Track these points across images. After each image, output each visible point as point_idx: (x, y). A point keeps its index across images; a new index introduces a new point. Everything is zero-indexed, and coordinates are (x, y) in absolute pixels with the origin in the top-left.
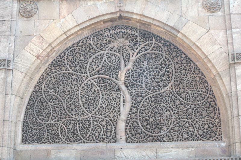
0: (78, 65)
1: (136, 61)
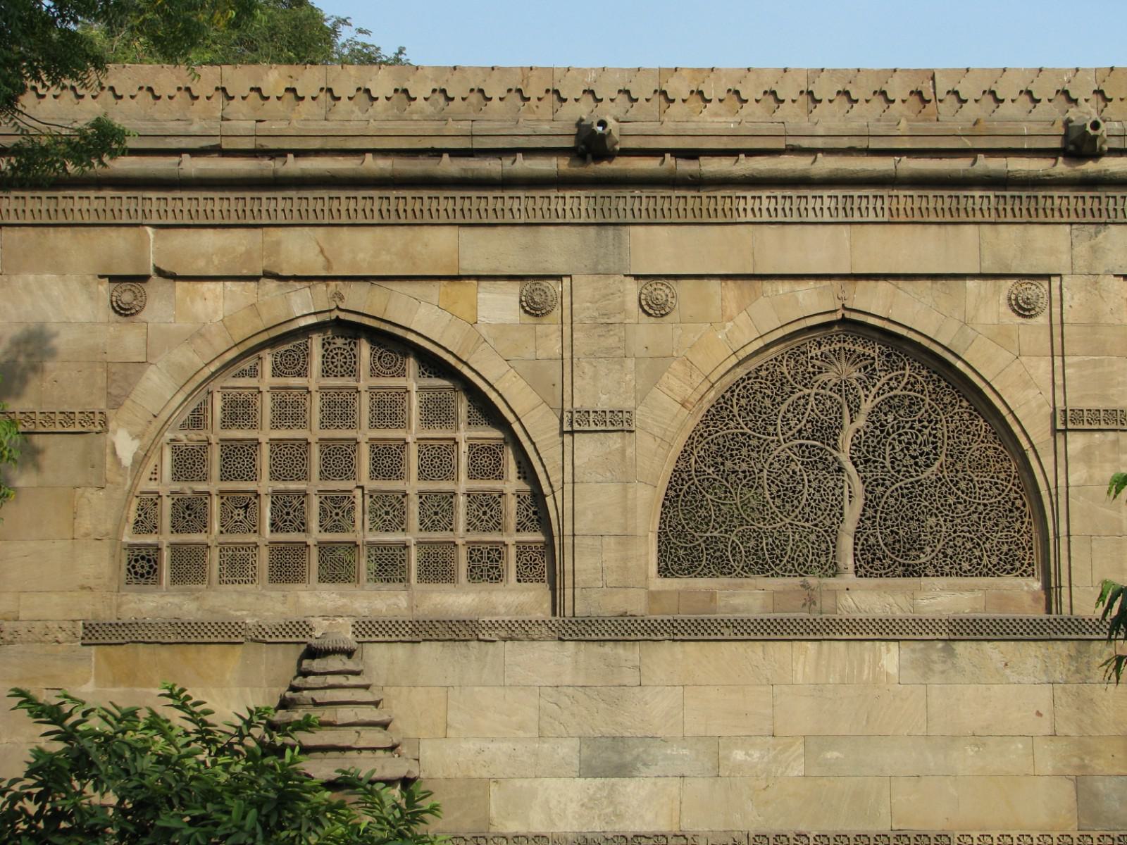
1: (873, 412)
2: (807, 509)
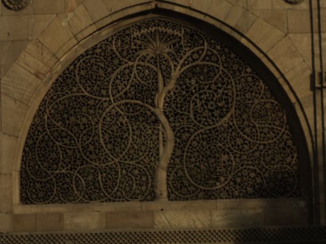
0: (95, 84)
1: (180, 77)
2: (132, 151)
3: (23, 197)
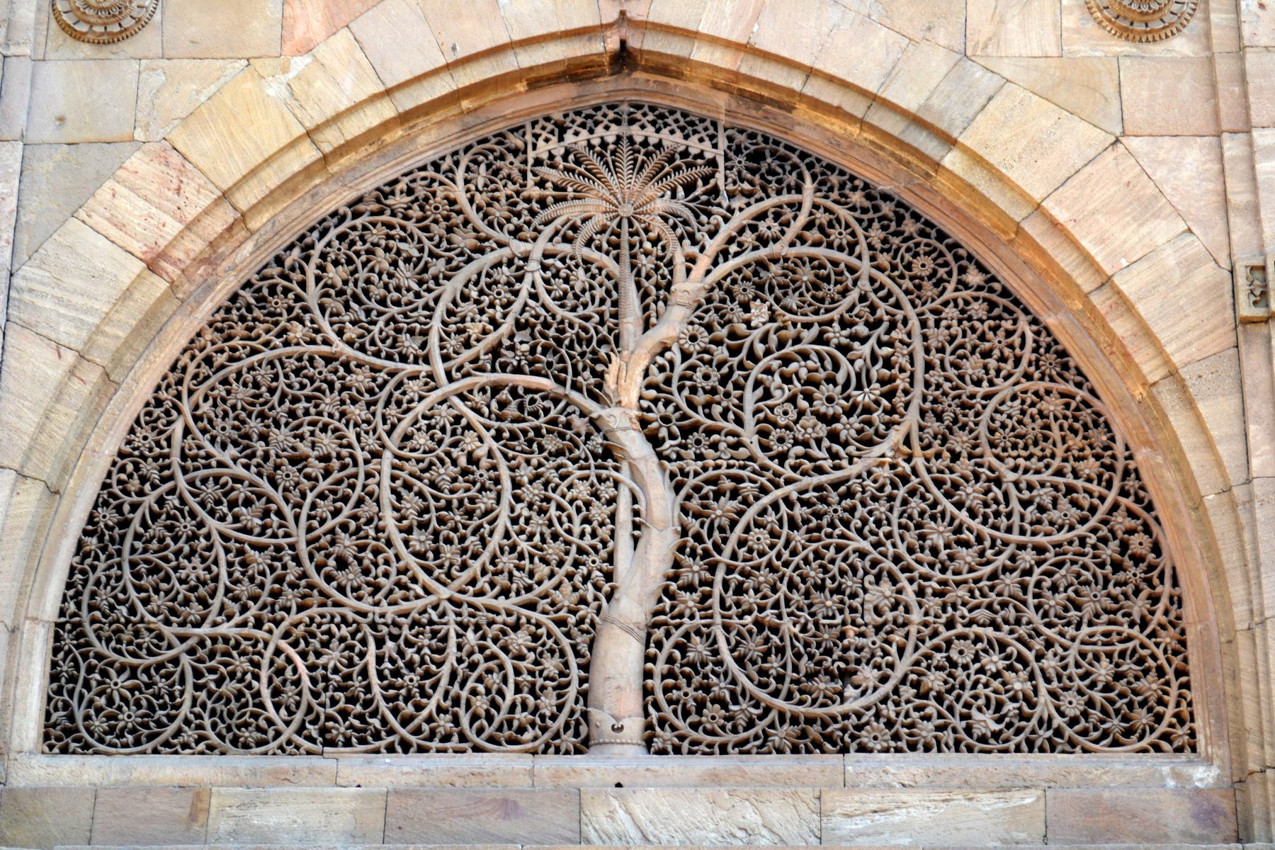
0: (380, 314)
3: (54, 726)
